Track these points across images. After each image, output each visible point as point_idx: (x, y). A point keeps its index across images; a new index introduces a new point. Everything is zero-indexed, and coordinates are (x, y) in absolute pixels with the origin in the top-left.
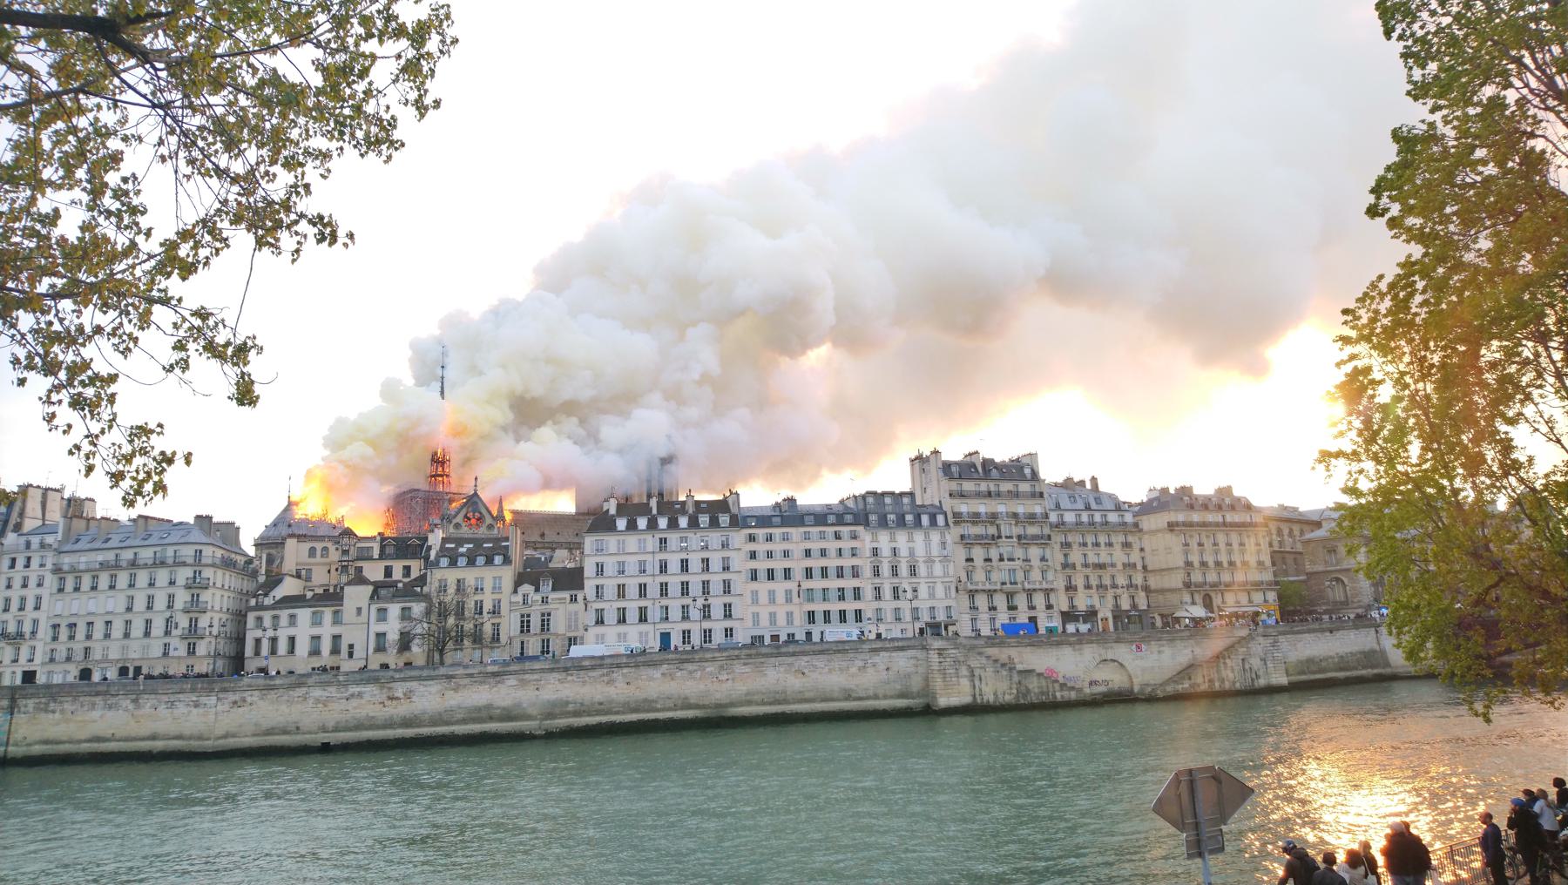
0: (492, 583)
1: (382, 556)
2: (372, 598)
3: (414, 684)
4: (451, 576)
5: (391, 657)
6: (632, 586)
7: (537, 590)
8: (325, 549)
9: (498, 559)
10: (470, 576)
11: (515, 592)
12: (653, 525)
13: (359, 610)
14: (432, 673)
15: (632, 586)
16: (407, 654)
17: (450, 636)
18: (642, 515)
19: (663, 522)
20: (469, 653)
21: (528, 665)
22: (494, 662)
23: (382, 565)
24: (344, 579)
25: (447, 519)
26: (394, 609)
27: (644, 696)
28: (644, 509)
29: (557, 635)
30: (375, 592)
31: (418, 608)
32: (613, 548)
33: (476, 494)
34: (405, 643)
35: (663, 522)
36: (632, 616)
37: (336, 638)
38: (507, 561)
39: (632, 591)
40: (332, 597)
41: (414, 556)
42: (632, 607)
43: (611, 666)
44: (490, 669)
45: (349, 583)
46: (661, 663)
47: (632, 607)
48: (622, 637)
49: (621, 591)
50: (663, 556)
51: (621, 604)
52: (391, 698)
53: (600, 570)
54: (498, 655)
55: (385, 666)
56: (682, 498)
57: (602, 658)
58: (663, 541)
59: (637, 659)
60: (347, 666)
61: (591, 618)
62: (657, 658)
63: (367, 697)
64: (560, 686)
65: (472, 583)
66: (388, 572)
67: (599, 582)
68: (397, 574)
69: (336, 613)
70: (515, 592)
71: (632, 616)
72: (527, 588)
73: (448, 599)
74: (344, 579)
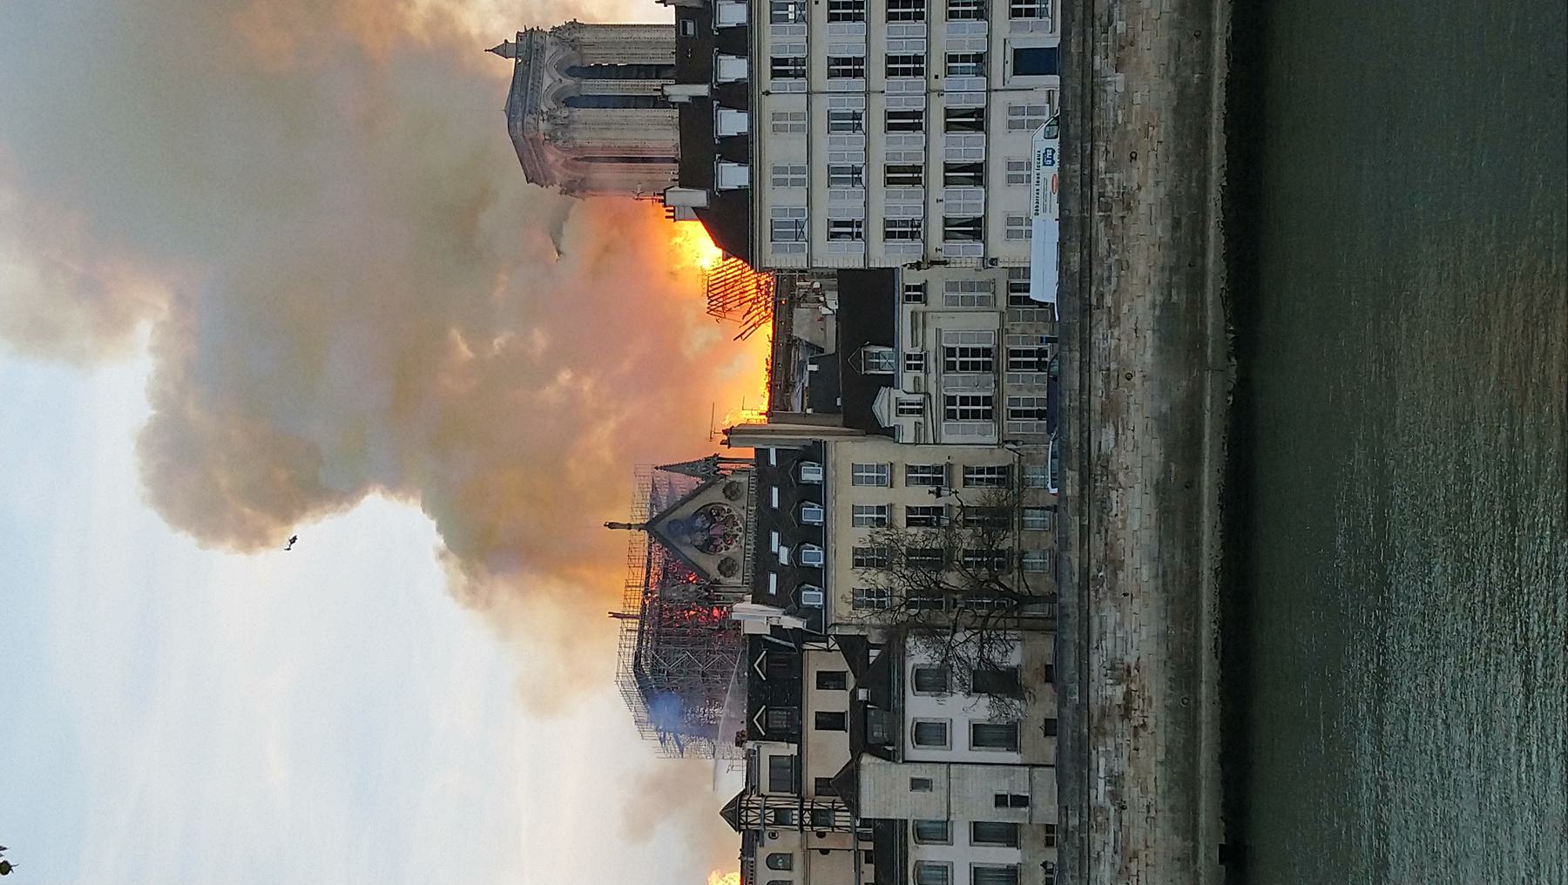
0: (867, 487)
1: (794, 735)
2: (889, 757)
3: (1096, 661)
4: (846, 579)
5: (1037, 709)
6: (887, 148)
7: (890, 381)
8: (772, 862)
9: (810, 475)
10: (848, 537)
11: (890, 433)
12: (739, 96)
13: (917, 784)
14: (1074, 620)
15: (887, 148)
16: (1026, 677)
17: (989, 581)
18: (711, 122)
19: (732, 69)
20: (1032, 539)
21: (1070, 402)
22: (1058, 480)
23: (813, 735)
24: (843, 818)
25: (711, 595)
26: (919, 707)
27: (1167, 118)
28: (695, 118)
29: (1002, 332)
30: (880, 751)
31: (919, 655)
32: (797, 197)
33: (648, 527)
34: (995, 682)
35: (732, 69)
36: (967, 147)
37: (981, 833)
38: (815, 453)
39: (906, 147)
40: (885, 844)
41: (795, 663)
42: (943, 147)
43: (1086, 201)
44: (1071, 490)
45: (854, 807)
46: (1088, 72)
47: (943, 147)
48: (1018, 173)
49: (904, 175)
50: (819, 68)
51: (936, 174)
52: (1126, 711)
53: (843, 229)
54: (1040, 475)
55: (1050, 728)
56: (667, 15)
57: (1064, 222)
58: (782, 68)
59: (1078, 129)
60: (1046, 809)
61: (966, 253)
62: (1075, 83)
63: (1120, 765)
64: (1128, 325)
65: (864, 531)
66: (828, 721)
67: (876, 230)
68: (837, 701)
69: (923, 835)
70: (890, 433)
71: (967, 147)
72: (883, 406)
73: (901, 587)
74: (843, 818)
